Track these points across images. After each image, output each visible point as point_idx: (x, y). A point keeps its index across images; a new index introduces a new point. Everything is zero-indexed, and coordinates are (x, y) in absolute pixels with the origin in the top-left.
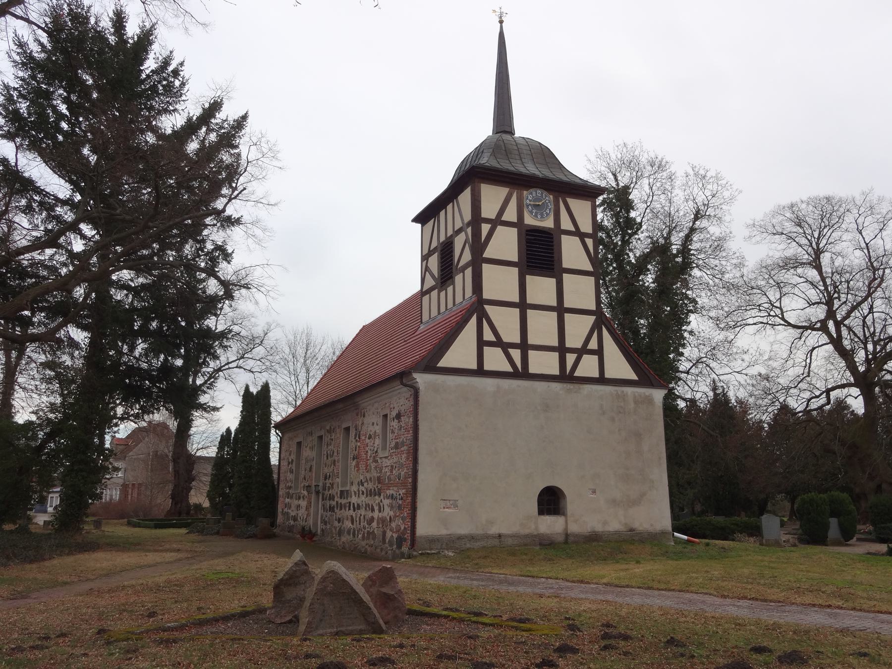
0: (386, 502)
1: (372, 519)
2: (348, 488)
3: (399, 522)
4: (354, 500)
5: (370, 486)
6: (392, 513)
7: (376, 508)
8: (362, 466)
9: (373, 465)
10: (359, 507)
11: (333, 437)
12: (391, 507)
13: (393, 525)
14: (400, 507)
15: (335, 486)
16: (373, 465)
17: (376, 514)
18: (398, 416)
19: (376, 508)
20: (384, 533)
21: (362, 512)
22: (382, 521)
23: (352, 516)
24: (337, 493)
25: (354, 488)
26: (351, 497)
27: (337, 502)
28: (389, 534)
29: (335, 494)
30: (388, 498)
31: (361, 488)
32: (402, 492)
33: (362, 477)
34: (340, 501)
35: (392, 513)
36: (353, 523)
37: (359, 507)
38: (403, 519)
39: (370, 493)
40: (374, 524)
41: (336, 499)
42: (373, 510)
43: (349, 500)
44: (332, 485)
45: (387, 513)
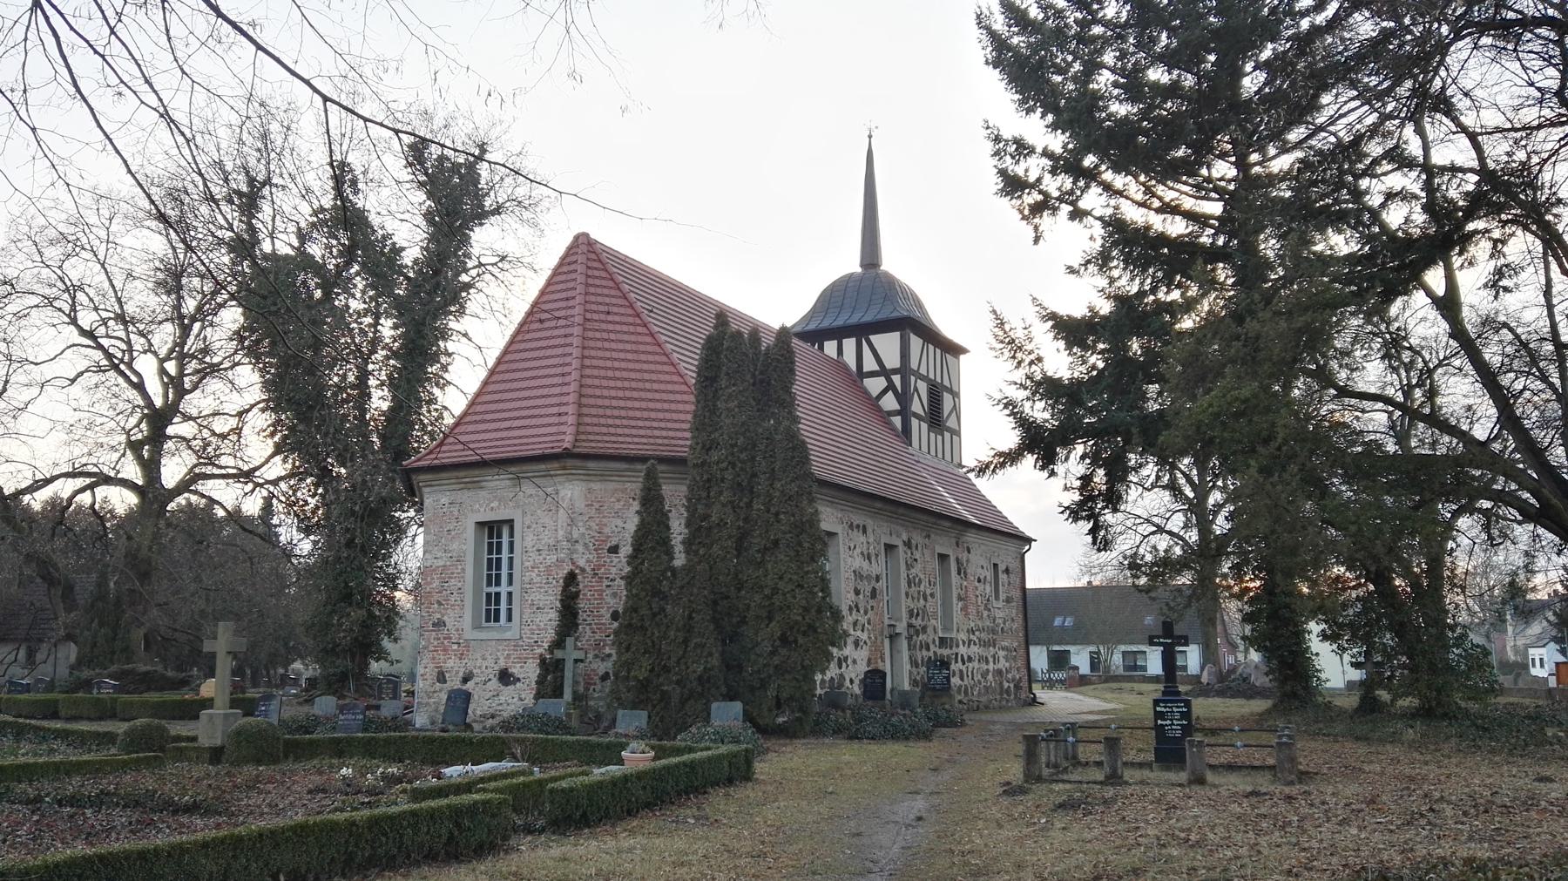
0: (1002, 653)
1: (988, 670)
2: (954, 635)
3: (1014, 672)
4: (963, 650)
5: (984, 636)
6: (1007, 665)
7: (991, 660)
8: (972, 609)
9: (985, 613)
10: (970, 659)
11: (917, 557)
12: (1006, 658)
13: (1010, 676)
14: (1014, 658)
15: (929, 630)
16: (985, 613)
17: (991, 666)
18: (1007, 571)
19: (991, 660)
20: (1001, 683)
21: (976, 664)
22: (999, 672)
23: (961, 671)
24: (934, 641)
25: (963, 636)
26: (958, 646)
27: (935, 653)
28: (1006, 685)
29: (930, 641)
30: (1003, 649)
31: (972, 637)
32: (1015, 644)
33: (972, 625)
34: (939, 652)
35: (1007, 665)
36: (962, 679)
37: (970, 659)
38: (1018, 669)
39: (986, 644)
40: (990, 677)
41: (932, 646)
42: (987, 662)
43: (955, 650)
44: (924, 629)
45: (1003, 664)
